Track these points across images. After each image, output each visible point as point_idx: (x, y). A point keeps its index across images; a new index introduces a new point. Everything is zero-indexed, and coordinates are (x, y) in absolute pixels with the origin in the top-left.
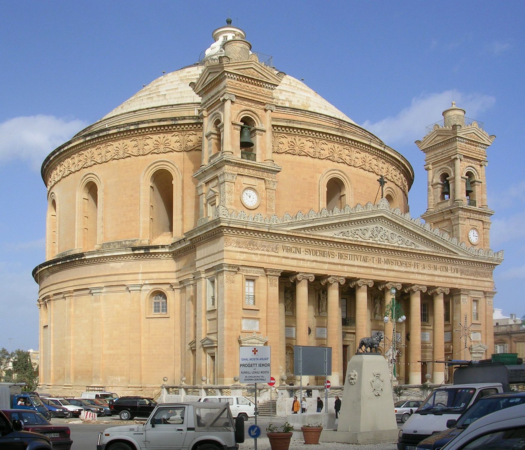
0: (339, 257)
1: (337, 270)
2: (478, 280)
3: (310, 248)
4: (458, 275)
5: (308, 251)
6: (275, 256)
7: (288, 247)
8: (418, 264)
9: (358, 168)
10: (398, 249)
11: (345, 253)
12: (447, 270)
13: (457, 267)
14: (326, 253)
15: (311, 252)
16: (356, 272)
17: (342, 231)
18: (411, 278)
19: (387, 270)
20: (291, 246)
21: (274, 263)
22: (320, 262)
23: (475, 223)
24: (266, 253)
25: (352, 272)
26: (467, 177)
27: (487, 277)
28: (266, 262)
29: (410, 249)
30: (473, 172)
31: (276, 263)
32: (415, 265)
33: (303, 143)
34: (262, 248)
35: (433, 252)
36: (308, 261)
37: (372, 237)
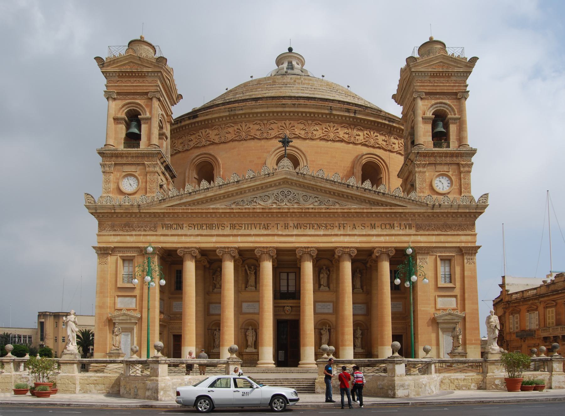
0: (232, 228)
2: (448, 235)
3: (195, 223)
4: (413, 231)
5: (194, 226)
7: (168, 224)
8: (345, 225)
10: (307, 211)
11: (239, 223)
12: (392, 227)
13: (410, 222)
14: (214, 225)
15: (196, 227)
16: (253, 241)
17: (236, 200)
18: (333, 241)
19: (297, 235)
20: (172, 223)
21: (152, 241)
23: (445, 168)
25: (248, 241)
27: (463, 230)
28: (142, 241)
29: (325, 209)
31: (153, 241)
32: (340, 226)
35: (363, 209)
37: (276, 203)
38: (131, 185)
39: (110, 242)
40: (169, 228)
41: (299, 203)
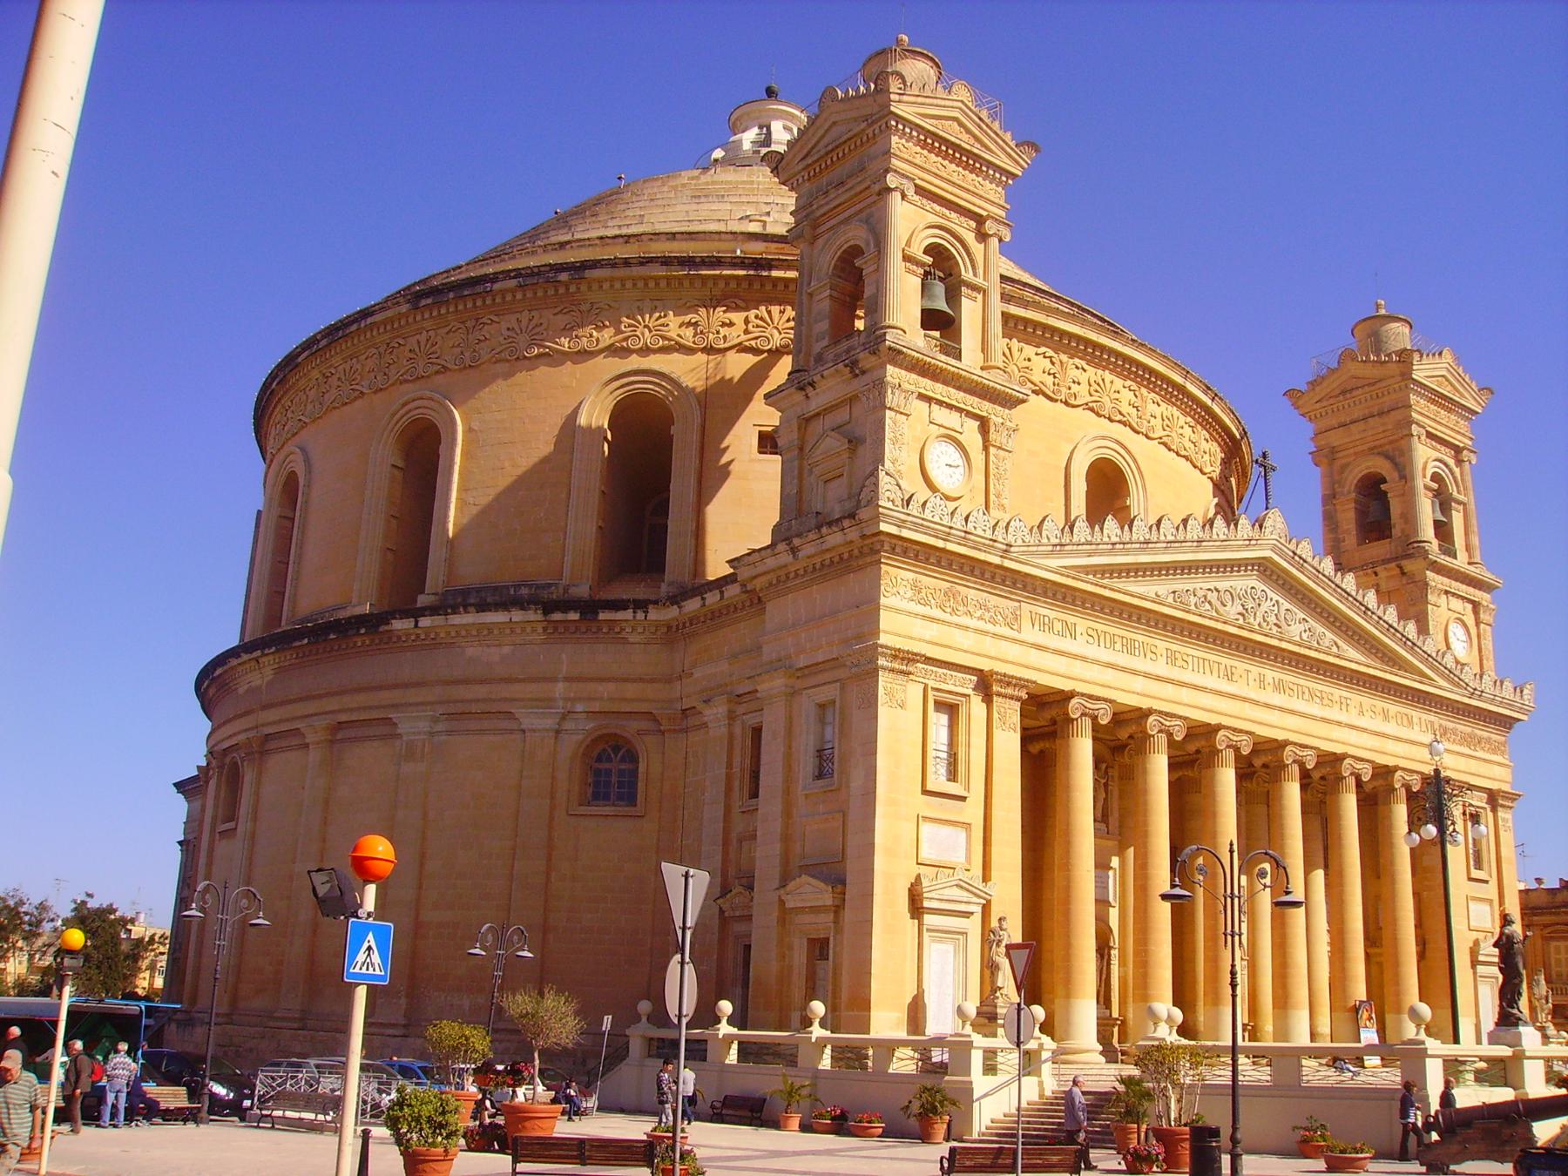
1: (1162, 697)
6: (1015, 640)
8: (1348, 701)
9: (1156, 442)
18: (1334, 738)
21: (1010, 659)
22: (1124, 670)
24: (989, 627)
26: (1435, 486)
30: (1444, 475)
33: (1029, 360)
34: (979, 613)
36: (1096, 662)
38: (950, 466)
39: (911, 638)
40: (1046, 627)
41: (1280, 627)
